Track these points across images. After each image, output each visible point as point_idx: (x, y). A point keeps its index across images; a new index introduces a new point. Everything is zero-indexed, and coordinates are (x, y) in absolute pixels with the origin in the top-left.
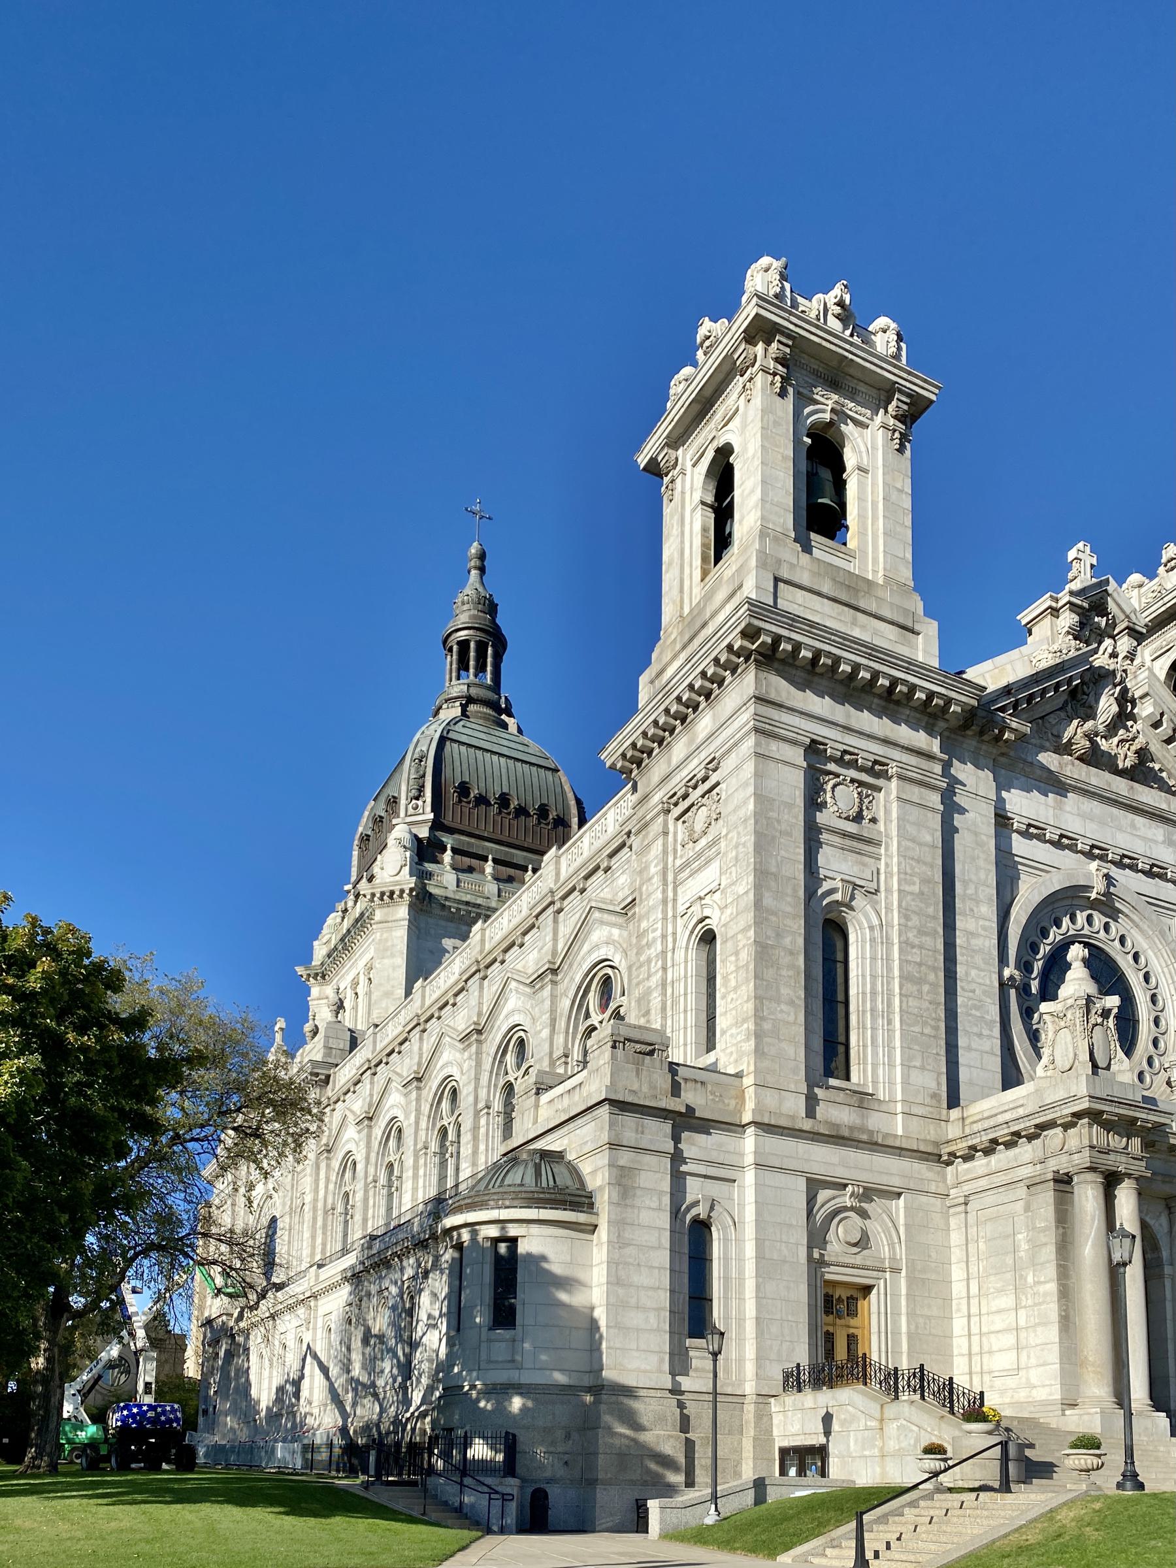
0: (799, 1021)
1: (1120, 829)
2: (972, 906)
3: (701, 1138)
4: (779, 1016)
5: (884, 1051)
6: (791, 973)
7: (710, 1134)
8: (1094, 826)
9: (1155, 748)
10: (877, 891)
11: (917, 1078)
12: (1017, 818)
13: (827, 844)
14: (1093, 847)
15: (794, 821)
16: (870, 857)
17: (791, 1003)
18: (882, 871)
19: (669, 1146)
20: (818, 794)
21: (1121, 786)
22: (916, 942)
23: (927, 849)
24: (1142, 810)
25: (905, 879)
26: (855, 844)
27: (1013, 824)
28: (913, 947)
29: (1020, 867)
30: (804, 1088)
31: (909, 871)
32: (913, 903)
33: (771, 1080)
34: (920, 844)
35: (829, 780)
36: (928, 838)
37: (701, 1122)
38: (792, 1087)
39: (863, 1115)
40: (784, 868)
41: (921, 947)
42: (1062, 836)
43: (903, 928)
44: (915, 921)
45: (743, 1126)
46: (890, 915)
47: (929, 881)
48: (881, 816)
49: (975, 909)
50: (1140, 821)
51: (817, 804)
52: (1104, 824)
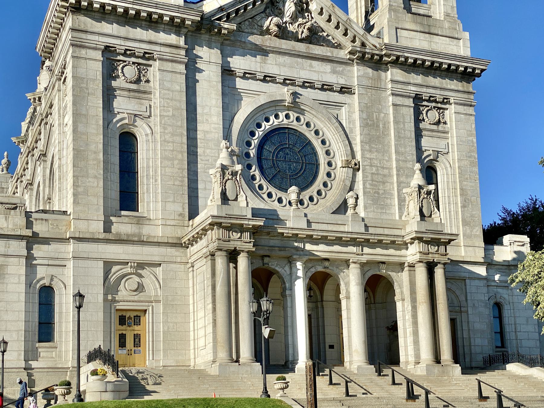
0: (99, 186)
1: (303, 69)
2: (207, 118)
3: (45, 247)
4: (88, 184)
5: (153, 195)
6: (95, 162)
7: (50, 244)
8: (286, 69)
9: (322, 24)
10: (149, 117)
11: (171, 207)
12: (237, 70)
13: (120, 96)
14: (285, 79)
15: (96, 87)
16: (146, 100)
17: (96, 177)
18: (152, 107)
19: (25, 252)
20: (113, 71)
21: (302, 47)
22: (171, 140)
23: (177, 93)
24: (315, 58)
25: (164, 110)
26: (136, 94)
27: (236, 73)
28: (169, 142)
29: (242, 94)
30: (102, 218)
31: (166, 105)
32: (168, 121)
33: (82, 216)
34: (173, 91)
35: (120, 64)
36: (178, 88)
37: (45, 239)
38: (96, 218)
39: (140, 228)
40: (90, 111)
41: (173, 142)
42: (265, 76)
43: (163, 134)
44: (170, 129)
45: (68, 239)
46: (156, 128)
47: (178, 109)
48: (151, 79)
49: (209, 120)
50: (315, 63)
51: (113, 77)
52: (292, 67)
